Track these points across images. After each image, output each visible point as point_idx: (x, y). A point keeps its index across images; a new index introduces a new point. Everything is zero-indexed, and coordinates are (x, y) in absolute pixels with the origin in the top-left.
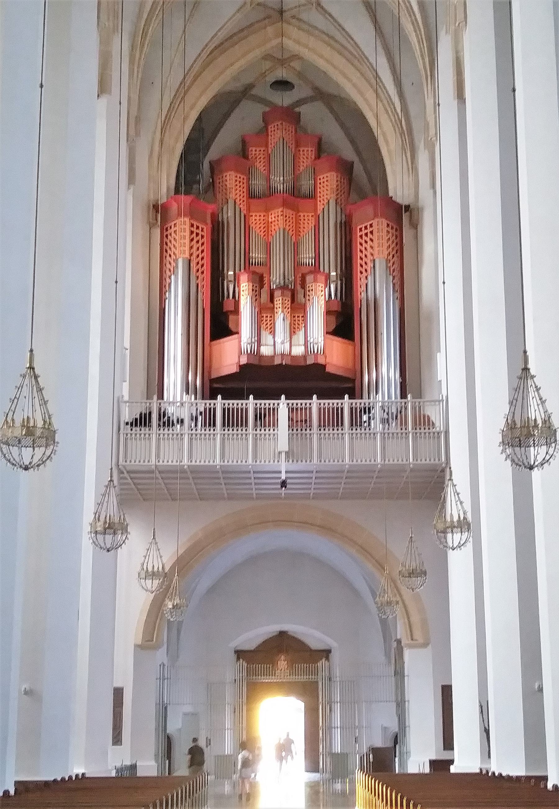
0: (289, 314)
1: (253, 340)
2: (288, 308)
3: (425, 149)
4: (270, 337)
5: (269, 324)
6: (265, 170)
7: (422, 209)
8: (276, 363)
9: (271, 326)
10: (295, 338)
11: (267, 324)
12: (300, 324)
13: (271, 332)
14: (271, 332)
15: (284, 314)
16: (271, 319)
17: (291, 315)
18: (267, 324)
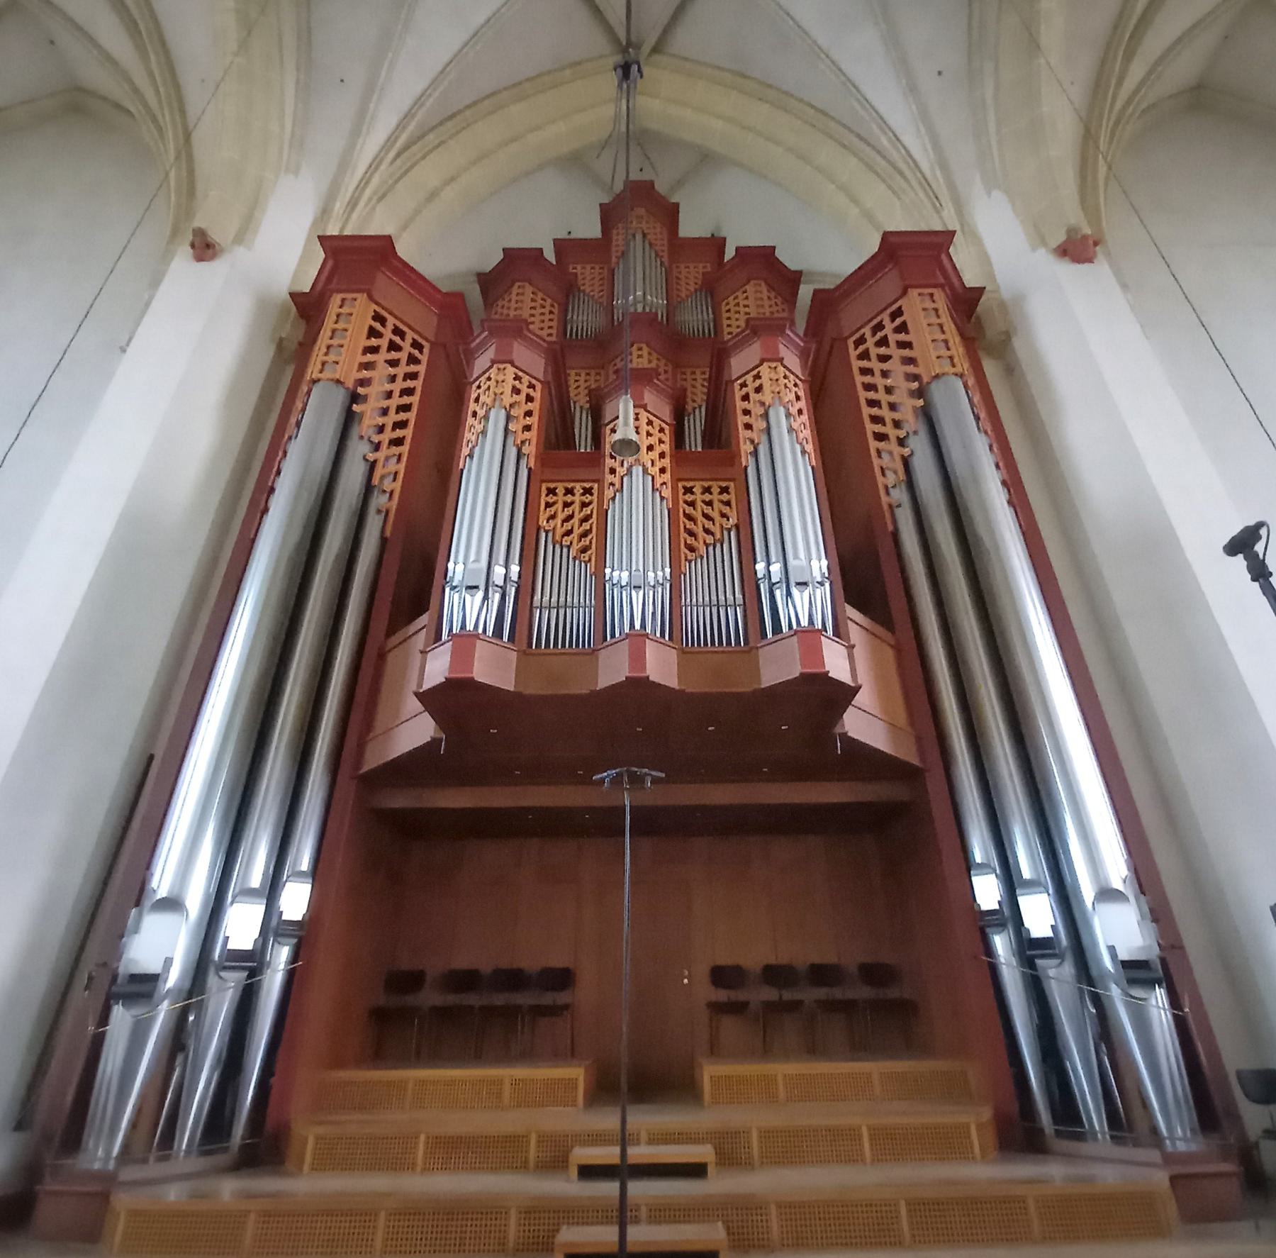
0: (667, 477)
1: (499, 571)
2: (662, 455)
3: (989, 194)
4: (579, 573)
5: (576, 521)
6: (602, 297)
7: (1020, 299)
8: (605, 681)
9: (586, 526)
10: (697, 573)
11: (570, 517)
12: (715, 515)
13: (584, 550)
14: (584, 550)
15: (645, 471)
16: (587, 498)
17: (676, 480)
18: (569, 518)
